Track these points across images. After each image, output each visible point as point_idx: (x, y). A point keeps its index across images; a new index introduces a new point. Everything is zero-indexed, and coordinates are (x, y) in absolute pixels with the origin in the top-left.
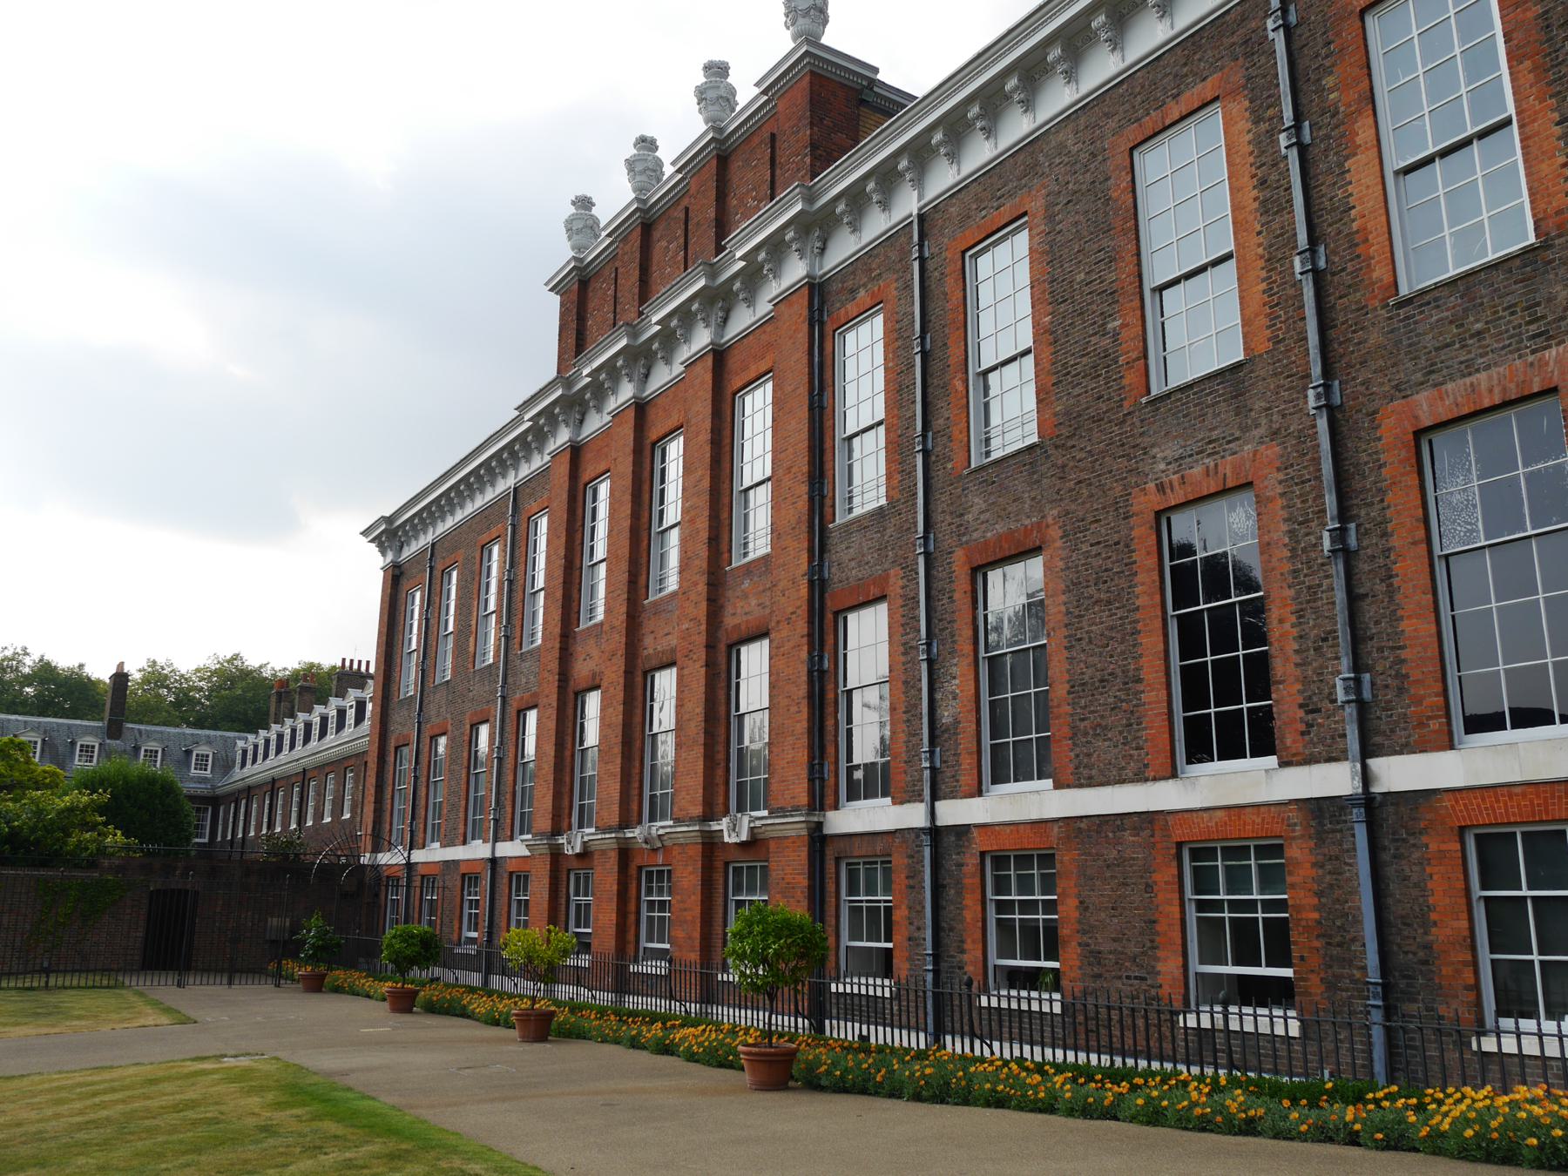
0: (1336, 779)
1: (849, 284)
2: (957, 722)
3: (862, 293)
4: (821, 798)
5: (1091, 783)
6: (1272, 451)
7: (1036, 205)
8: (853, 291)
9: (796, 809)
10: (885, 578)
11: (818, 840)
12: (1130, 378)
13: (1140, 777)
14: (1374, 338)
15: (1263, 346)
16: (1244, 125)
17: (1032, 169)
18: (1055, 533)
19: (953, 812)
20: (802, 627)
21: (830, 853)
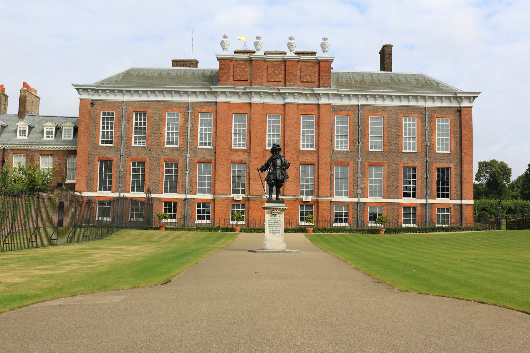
0: (423, 201)
1: (340, 108)
2: (364, 187)
3: (343, 112)
4: (332, 196)
5: (390, 198)
6: (420, 164)
7: (386, 116)
8: (341, 110)
9: (327, 197)
10: (349, 162)
11: (331, 202)
12: (400, 148)
13: (398, 198)
14: (433, 156)
15: (420, 151)
16: (420, 123)
17: (384, 110)
18: (386, 165)
19: (362, 200)
20: (329, 166)
21: (332, 204)
